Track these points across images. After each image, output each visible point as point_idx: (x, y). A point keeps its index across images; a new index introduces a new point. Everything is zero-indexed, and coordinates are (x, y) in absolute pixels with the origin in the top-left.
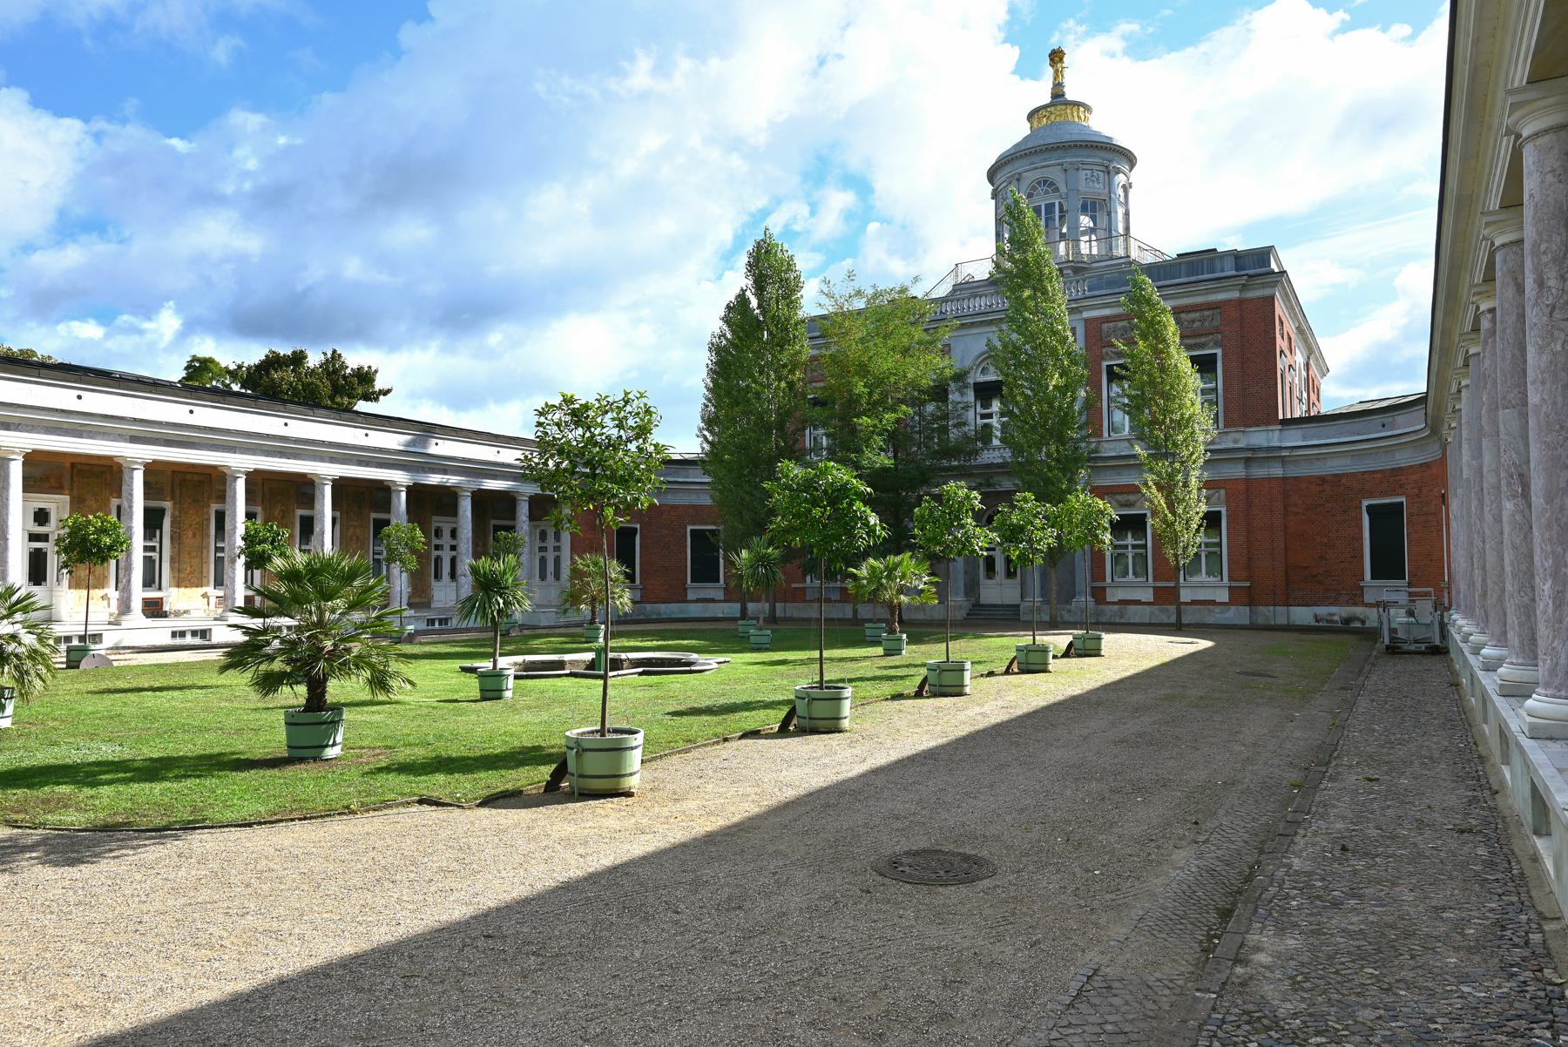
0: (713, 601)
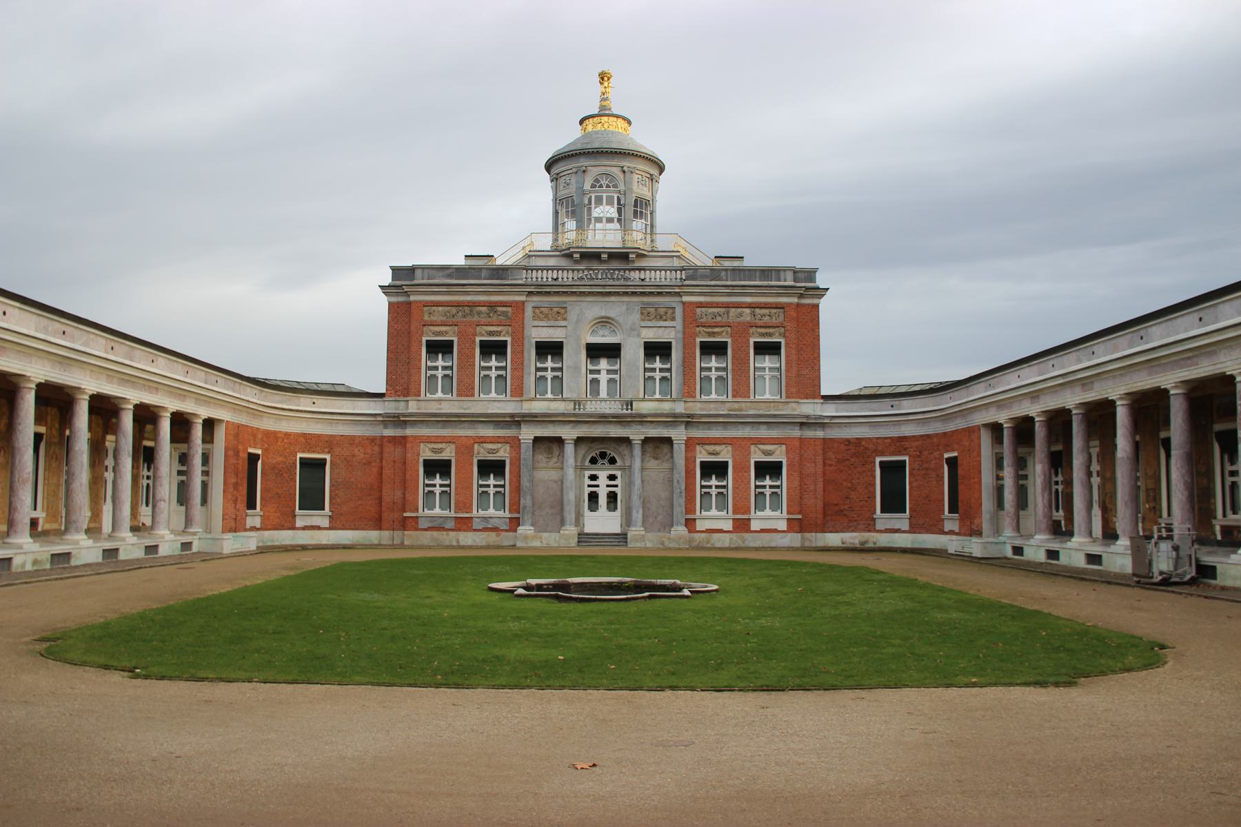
0: (318, 528)
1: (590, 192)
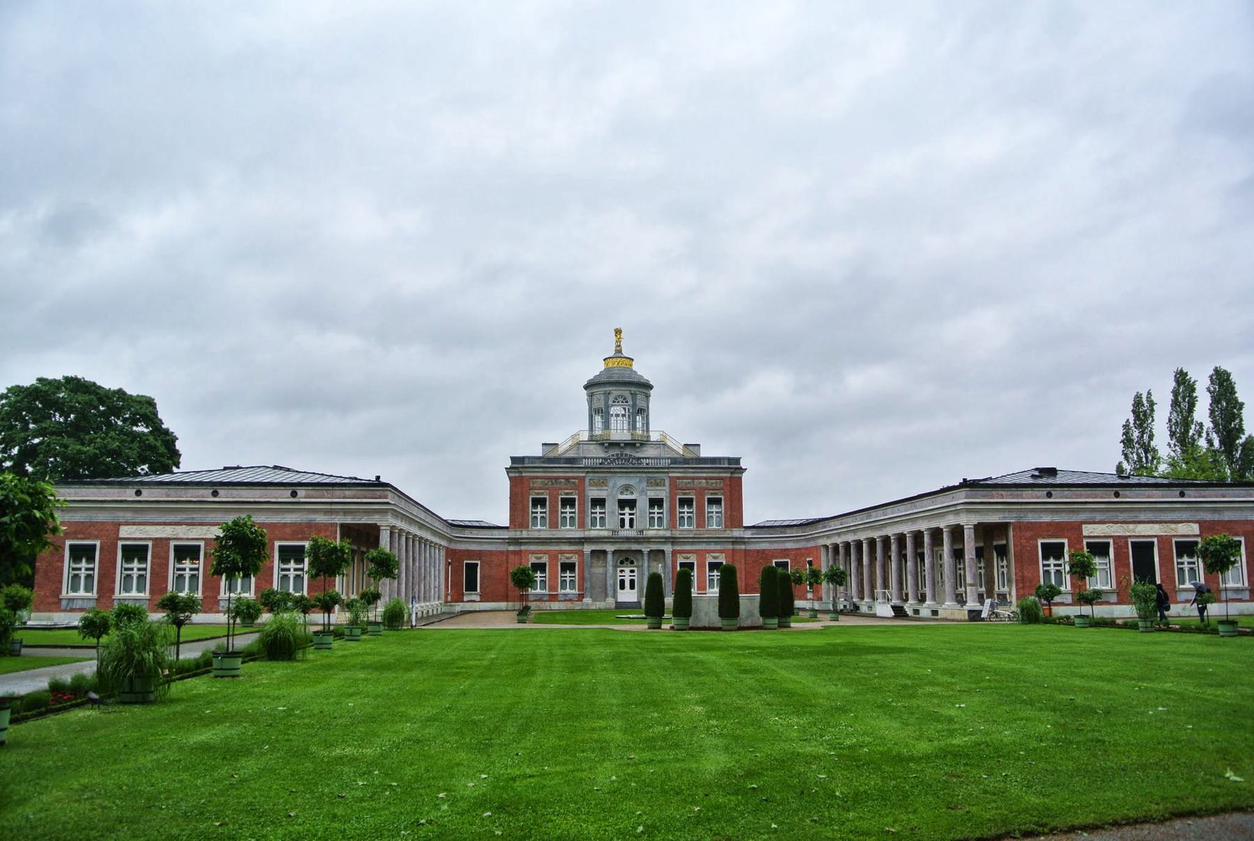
0: (474, 601)
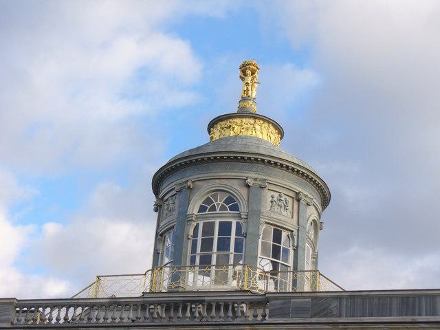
1: (198, 218)
